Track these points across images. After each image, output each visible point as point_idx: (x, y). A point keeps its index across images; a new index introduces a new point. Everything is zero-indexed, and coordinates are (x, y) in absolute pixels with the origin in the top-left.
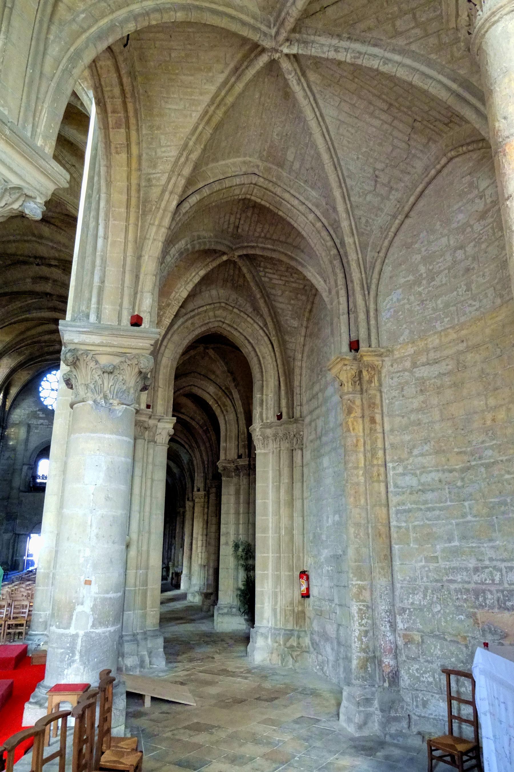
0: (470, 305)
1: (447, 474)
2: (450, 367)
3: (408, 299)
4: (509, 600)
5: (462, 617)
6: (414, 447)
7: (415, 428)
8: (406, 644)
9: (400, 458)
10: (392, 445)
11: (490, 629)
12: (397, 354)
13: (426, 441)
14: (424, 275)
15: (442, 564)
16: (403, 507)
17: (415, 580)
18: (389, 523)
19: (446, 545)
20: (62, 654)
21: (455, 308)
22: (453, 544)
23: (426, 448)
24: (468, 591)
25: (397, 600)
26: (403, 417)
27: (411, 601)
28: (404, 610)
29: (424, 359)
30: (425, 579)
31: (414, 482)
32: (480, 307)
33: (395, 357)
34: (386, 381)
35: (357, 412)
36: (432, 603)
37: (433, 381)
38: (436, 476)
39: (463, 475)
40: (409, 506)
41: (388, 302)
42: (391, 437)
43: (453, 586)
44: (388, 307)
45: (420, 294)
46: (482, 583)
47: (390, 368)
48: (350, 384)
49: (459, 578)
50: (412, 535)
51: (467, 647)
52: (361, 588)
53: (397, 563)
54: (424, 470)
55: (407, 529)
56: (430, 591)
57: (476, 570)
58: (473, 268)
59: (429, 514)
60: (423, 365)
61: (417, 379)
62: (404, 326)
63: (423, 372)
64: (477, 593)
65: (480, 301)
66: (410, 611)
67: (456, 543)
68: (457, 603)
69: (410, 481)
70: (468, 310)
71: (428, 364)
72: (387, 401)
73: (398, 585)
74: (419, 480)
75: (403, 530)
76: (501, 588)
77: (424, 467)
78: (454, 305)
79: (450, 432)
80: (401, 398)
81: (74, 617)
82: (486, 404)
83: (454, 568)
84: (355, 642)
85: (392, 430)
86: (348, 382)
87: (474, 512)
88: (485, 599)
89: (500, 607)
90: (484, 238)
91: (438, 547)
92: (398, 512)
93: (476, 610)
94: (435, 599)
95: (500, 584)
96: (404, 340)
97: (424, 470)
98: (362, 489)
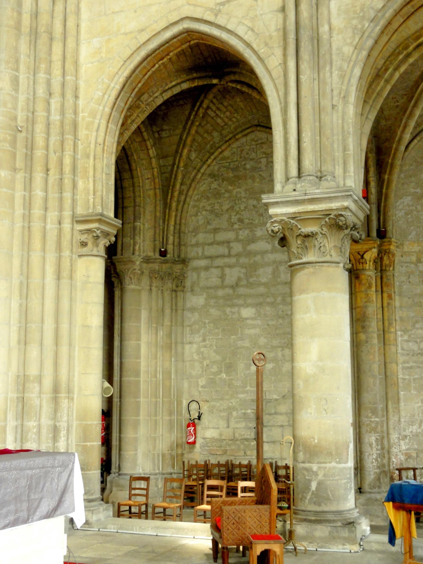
6: (417, 322)
7: (418, 308)
8: (407, 459)
9: (406, 329)
10: (401, 319)
12: (406, 249)
16: (408, 365)
17: (414, 416)
18: (397, 375)
20: (345, 483)
25: (402, 430)
26: (409, 298)
27: (410, 430)
28: (406, 437)
34: (397, 267)
35: (374, 289)
40: (411, 364)
41: (400, 204)
42: (400, 312)
44: (400, 207)
47: (401, 258)
50: (413, 385)
52: (377, 423)
53: (402, 404)
55: (409, 381)
62: (412, 228)
66: (410, 437)
72: (398, 283)
73: (402, 420)
74: (419, 346)
75: (407, 381)
80: (408, 284)
84: (372, 463)
85: (401, 307)
86: (370, 261)
92: (403, 368)
96: (412, 238)
98: (377, 348)
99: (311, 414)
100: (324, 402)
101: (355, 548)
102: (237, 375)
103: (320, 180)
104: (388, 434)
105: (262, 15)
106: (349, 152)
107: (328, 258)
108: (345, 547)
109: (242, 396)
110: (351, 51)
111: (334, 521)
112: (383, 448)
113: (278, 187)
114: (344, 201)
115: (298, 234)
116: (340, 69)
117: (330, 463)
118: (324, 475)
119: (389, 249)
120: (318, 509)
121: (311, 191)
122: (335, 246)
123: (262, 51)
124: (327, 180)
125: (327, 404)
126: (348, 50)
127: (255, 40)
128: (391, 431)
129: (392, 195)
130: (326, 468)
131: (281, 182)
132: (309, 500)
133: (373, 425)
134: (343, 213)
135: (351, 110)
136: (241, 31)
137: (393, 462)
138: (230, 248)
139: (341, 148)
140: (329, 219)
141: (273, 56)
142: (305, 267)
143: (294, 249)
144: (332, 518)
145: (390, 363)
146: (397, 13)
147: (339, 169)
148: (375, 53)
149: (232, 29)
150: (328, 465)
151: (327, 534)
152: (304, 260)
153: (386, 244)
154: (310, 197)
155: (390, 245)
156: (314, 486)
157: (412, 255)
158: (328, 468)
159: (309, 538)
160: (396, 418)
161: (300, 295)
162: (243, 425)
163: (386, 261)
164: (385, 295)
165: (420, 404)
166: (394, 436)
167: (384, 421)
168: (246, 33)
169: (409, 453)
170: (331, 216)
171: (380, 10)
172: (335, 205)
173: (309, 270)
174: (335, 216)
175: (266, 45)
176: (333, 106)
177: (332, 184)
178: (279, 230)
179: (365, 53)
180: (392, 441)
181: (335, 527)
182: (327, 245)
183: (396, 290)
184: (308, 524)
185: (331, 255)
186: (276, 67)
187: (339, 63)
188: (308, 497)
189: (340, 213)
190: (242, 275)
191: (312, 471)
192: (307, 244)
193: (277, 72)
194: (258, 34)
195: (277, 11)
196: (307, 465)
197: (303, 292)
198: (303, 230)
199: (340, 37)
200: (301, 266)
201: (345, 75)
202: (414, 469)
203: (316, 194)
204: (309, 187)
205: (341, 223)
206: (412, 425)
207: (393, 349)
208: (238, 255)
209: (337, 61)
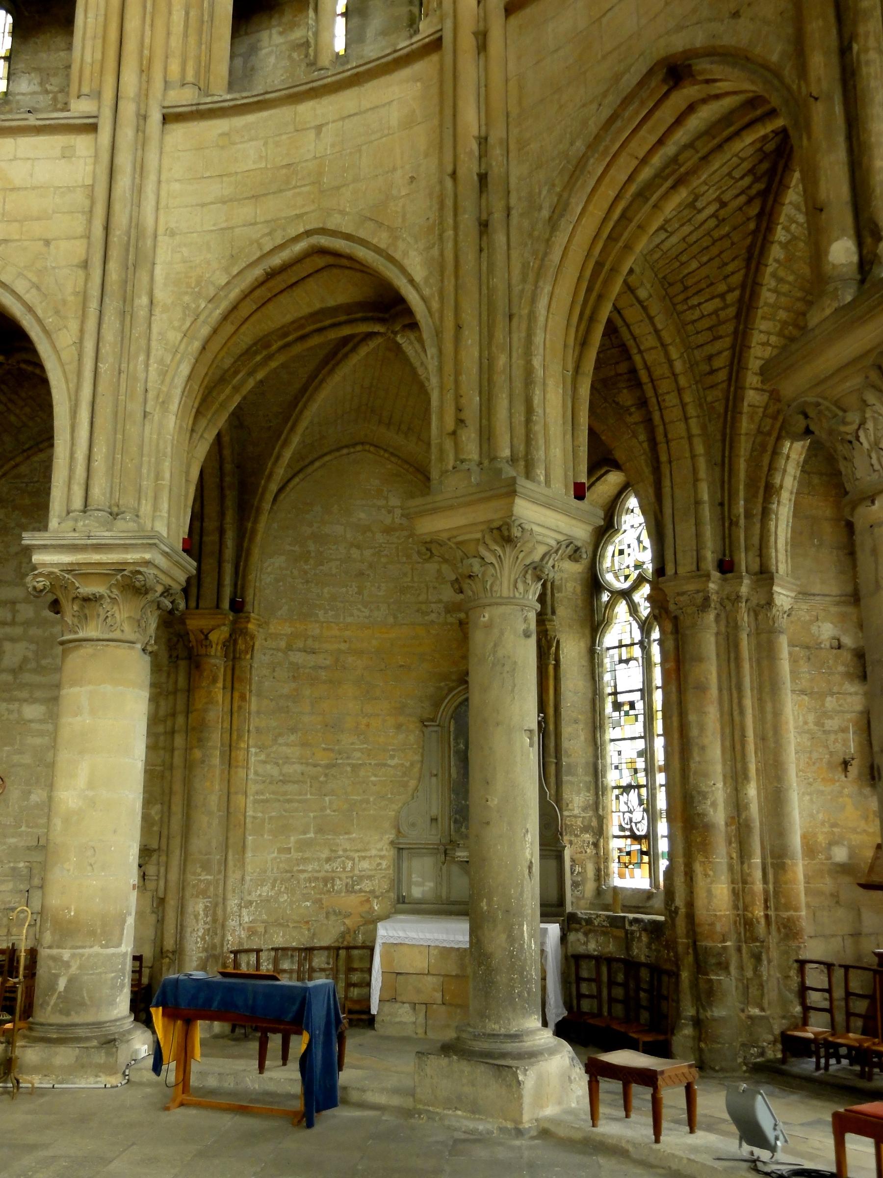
0: (359, 610)
1: (310, 768)
2: (328, 662)
3: (292, 572)
4: (358, 884)
5: (308, 904)
6: (280, 735)
8: (249, 937)
10: (258, 730)
11: (334, 911)
12: (272, 629)
13: (293, 730)
14: (313, 554)
15: (295, 855)
16: (262, 797)
17: (265, 872)
18: (245, 812)
19: (302, 837)
20: (113, 978)
21: (342, 605)
22: (308, 836)
23: (293, 738)
24: (317, 879)
25: (246, 893)
26: (271, 700)
27: (259, 892)
28: (251, 903)
29: (300, 644)
30: (275, 870)
31: (274, 771)
32: (370, 616)
33: (270, 631)
34: (258, 655)
35: (220, 684)
36: (279, 893)
37: (307, 671)
38: (298, 768)
39: (327, 771)
43: (303, 876)
45: (306, 572)
46: (333, 871)
48: (219, 648)
49: (310, 868)
50: (267, 826)
51: (309, 930)
52: (209, 883)
53: (249, 854)
54: (287, 760)
56: (278, 882)
57: (328, 860)
58: (368, 575)
59: (287, 806)
60: (299, 650)
61: (291, 663)
62: (284, 601)
63: (297, 657)
64: (325, 881)
65: (371, 611)
66: (257, 904)
67: (311, 835)
68: (305, 892)
69: (272, 770)
70: (355, 612)
71: (305, 651)
73: (248, 878)
76: (351, 875)
77: (287, 758)
78: (342, 602)
79: (319, 727)
81: (125, 932)
82: (362, 710)
83: (306, 858)
84: (197, 943)
85: (258, 712)
86: (217, 644)
87: (335, 807)
88: (333, 886)
89: (347, 891)
90: (385, 552)
91: (292, 838)
92: (256, 802)
93: (323, 896)
94: (282, 890)
95: (350, 871)
97: (287, 760)
98: (218, 772)
99: (69, 870)
100: (90, 853)
101: (115, 1080)
102: (8, 807)
103: (115, 519)
104: (224, 899)
105: (54, 268)
106: (163, 483)
107: (117, 635)
108: (99, 1079)
109: (12, 841)
110: (179, 338)
111: (87, 1039)
112: (215, 921)
113: (53, 523)
114: (145, 552)
115: (74, 596)
116: (161, 361)
117: (91, 947)
118: (80, 968)
119: (246, 628)
120: (65, 1020)
121: (98, 534)
122: (130, 617)
123: (50, 321)
124: (125, 519)
125: (94, 855)
126: (174, 336)
127: (41, 303)
128: (229, 895)
129: (256, 552)
130: (83, 955)
131: (59, 516)
132: (52, 1009)
133: (202, 886)
134: (142, 569)
135: (171, 422)
136: (20, 287)
137: (228, 941)
138: (14, 612)
139: (152, 475)
140: (122, 576)
141: (65, 330)
142: (81, 646)
143: (69, 619)
144: (84, 1035)
145: (236, 793)
146: (246, 296)
147: (146, 505)
148: (215, 347)
149: (7, 283)
150: (87, 951)
151: (72, 1060)
152: (81, 635)
153: (242, 620)
154: (95, 542)
155: (248, 622)
156: (62, 984)
157: (281, 639)
158: (86, 955)
159: (43, 1069)
160: (238, 875)
161: (71, 687)
162: (10, 886)
163: (241, 645)
164: (236, 695)
165: (275, 855)
166: (233, 903)
167: (219, 879)
168: (28, 292)
169: (253, 927)
170: (125, 573)
171: (222, 288)
172: (131, 557)
173: (87, 650)
174: (131, 572)
175: (57, 312)
176: (145, 414)
177: (132, 525)
178: (45, 588)
179: (197, 345)
180: (229, 909)
181: (87, 1048)
182: (117, 615)
183: (254, 687)
184: (45, 1045)
185: (122, 631)
186: (68, 346)
187: (160, 353)
188: (52, 1002)
189: (138, 569)
190: (30, 655)
191: (62, 961)
192: (87, 611)
193: (69, 354)
194: (45, 296)
195: (77, 266)
196: (55, 951)
197: (74, 683)
198: (81, 590)
199: (165, 316)
200: (77, 643)
201: (167, 371)
202: (258, 951)
203: (104, 538)
204: (96, 527)
205: (137, 584)
206: (262, 885)
207: (242, 773)
208: (27, 623)
209: (157, 350)
